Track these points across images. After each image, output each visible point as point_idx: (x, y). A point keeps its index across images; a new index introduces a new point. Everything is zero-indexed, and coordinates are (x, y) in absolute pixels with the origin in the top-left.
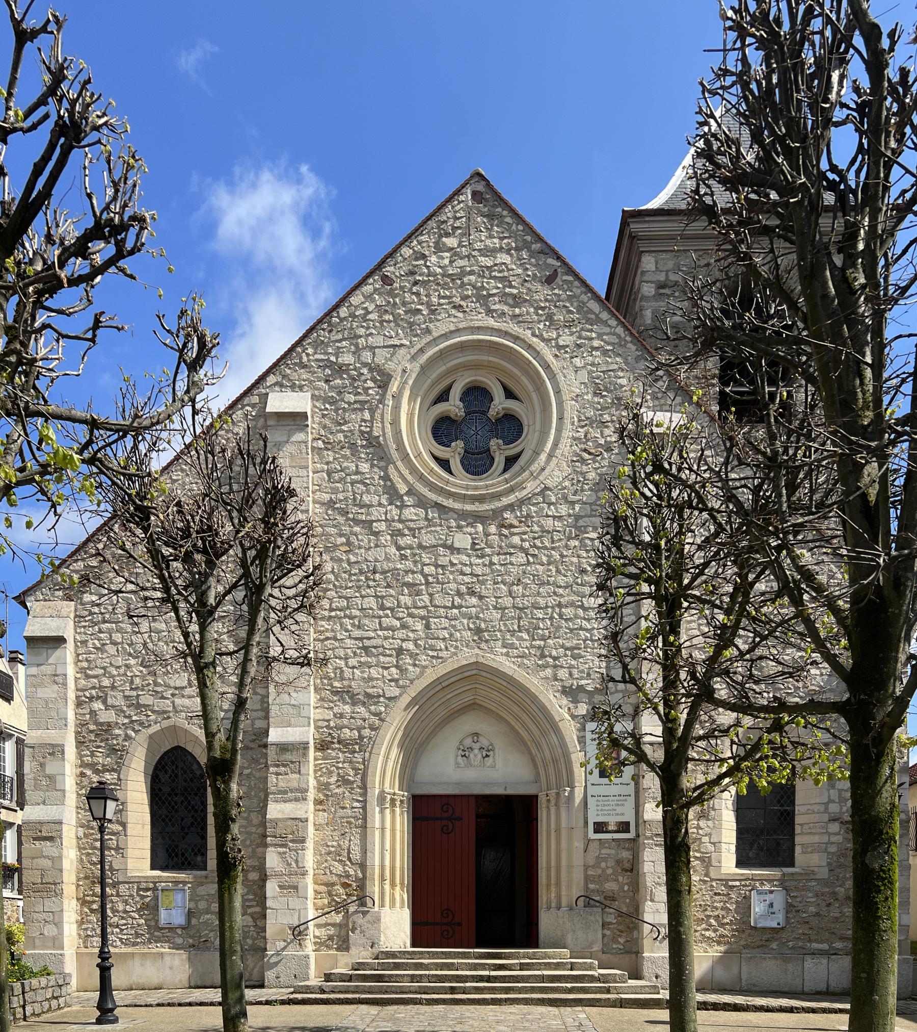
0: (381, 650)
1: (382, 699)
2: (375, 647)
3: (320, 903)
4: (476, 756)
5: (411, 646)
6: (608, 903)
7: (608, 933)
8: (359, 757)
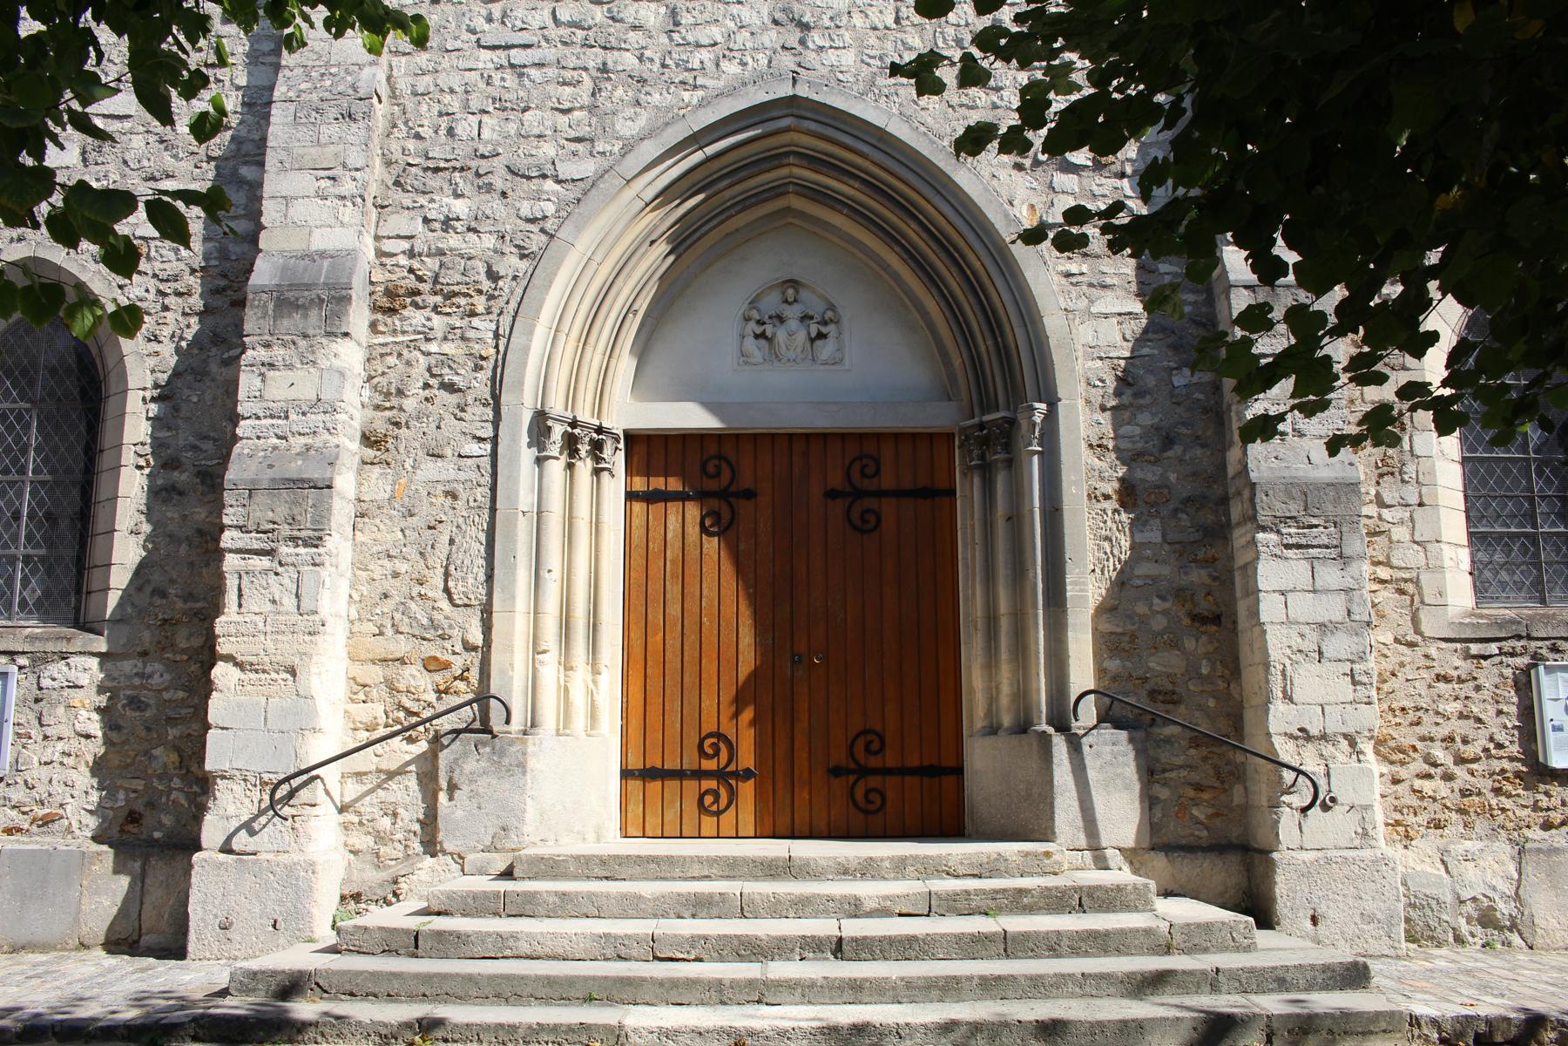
0: (552, 72)
1: (549, 185)
2: (540, 65)
3: (364, 713)
4: (792, 336)
5: (629, 60)
6: (1159, 709)
7: (1164, 793)
8: (484, 326)
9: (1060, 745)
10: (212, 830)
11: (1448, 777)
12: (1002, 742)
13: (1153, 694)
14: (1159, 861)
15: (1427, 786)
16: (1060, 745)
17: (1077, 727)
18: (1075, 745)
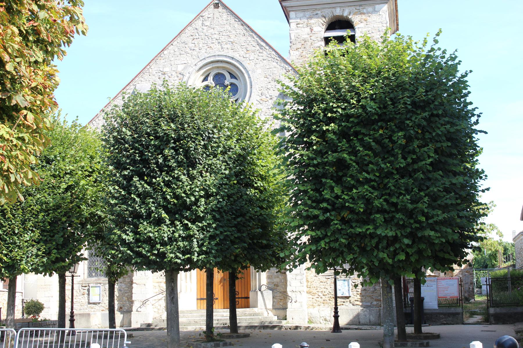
7: (275, 300)
9: (259, 293)
10: (134, 309)
11: (321, 298)
12: (253, 292)
13: (274, 285)
14: (274, 311)
15: (318, 299)
16: (259, 293)
17: (262, 290)
18: (262, 293)
